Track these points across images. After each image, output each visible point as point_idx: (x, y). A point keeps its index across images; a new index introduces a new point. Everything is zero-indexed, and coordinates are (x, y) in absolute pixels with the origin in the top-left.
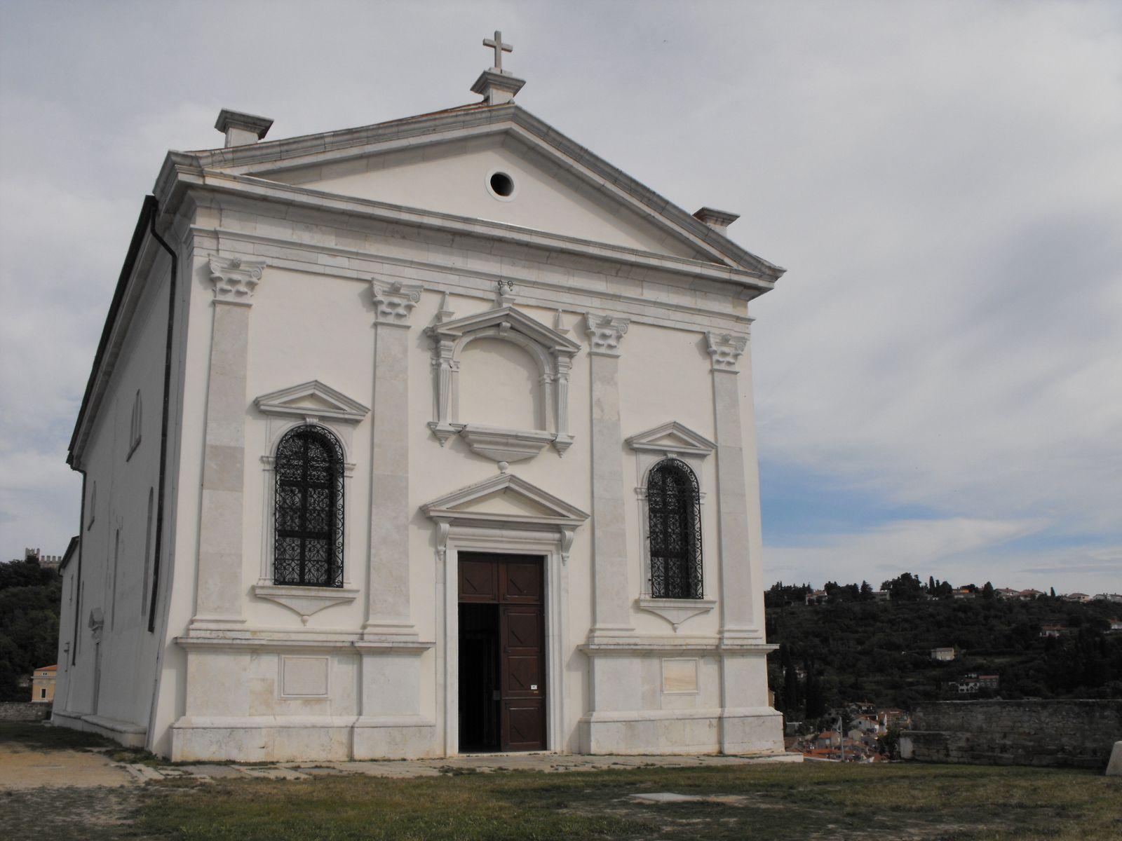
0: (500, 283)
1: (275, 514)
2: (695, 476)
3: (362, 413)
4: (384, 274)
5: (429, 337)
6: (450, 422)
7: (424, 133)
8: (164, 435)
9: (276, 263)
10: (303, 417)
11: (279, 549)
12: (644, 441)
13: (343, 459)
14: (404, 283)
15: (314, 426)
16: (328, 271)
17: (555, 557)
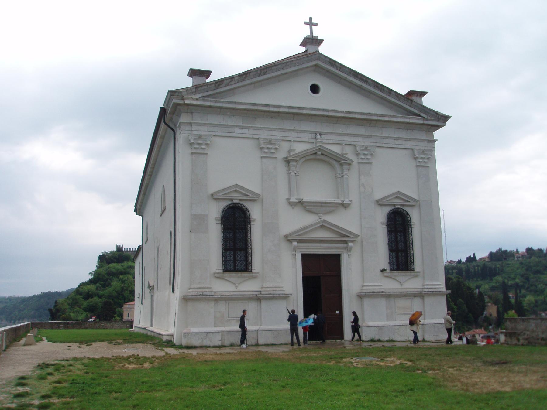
0: (316, 135)
1: (222, 242)
2: (409, 215)
3: (257, 197)
4: (264, 135)
5: (285, 161)
6: (296, 198)
8: (175, 209)
9: (217, 134)
10: (232, 200)
11: (224, 257)
12: (384, 201)
13: (250, 217)
14: (273, 139)
15: (237, 204)
16: (240, 135)
17: (345, 254)
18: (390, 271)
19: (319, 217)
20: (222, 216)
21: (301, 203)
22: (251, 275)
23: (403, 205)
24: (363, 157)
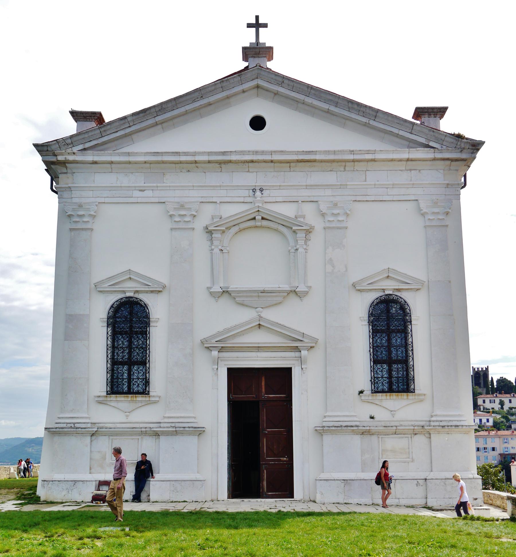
0: (254, 191)
7: (194, 101)
9: (107, 200)
12: (365, 284)
15: (132, 297)
16: (139, 200)
18: (372, 393)
19: (257, 312)
20: (108, 316)
21: (226, 292)
22: (147, 399)
23: (399, 290)
24: (331, 219)
